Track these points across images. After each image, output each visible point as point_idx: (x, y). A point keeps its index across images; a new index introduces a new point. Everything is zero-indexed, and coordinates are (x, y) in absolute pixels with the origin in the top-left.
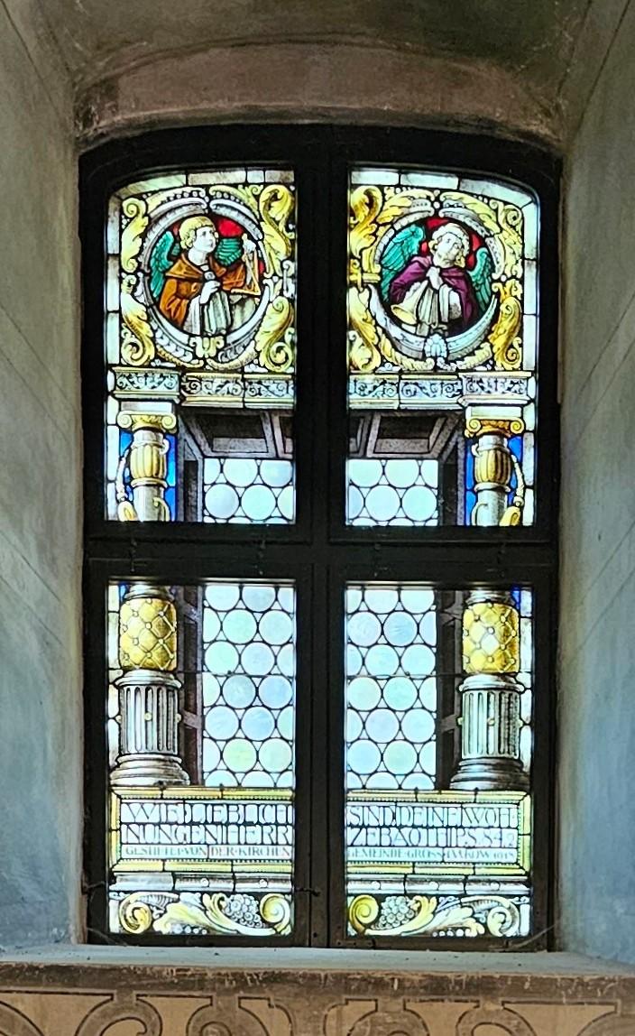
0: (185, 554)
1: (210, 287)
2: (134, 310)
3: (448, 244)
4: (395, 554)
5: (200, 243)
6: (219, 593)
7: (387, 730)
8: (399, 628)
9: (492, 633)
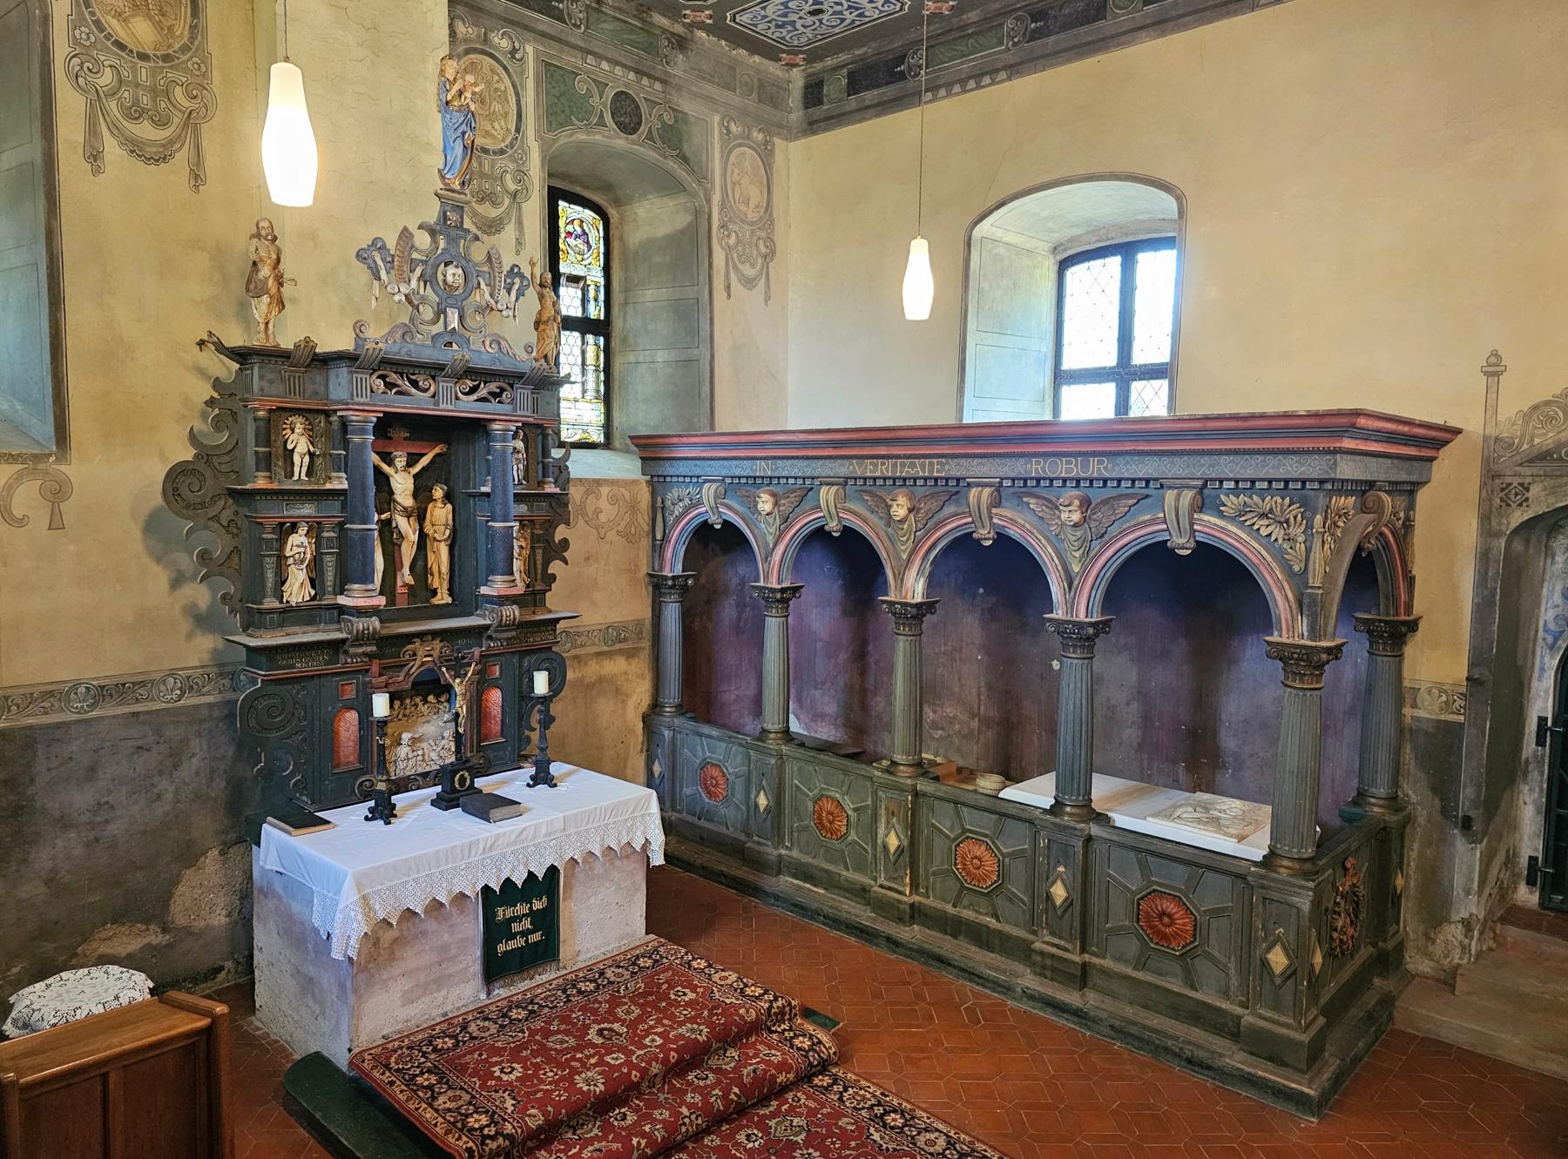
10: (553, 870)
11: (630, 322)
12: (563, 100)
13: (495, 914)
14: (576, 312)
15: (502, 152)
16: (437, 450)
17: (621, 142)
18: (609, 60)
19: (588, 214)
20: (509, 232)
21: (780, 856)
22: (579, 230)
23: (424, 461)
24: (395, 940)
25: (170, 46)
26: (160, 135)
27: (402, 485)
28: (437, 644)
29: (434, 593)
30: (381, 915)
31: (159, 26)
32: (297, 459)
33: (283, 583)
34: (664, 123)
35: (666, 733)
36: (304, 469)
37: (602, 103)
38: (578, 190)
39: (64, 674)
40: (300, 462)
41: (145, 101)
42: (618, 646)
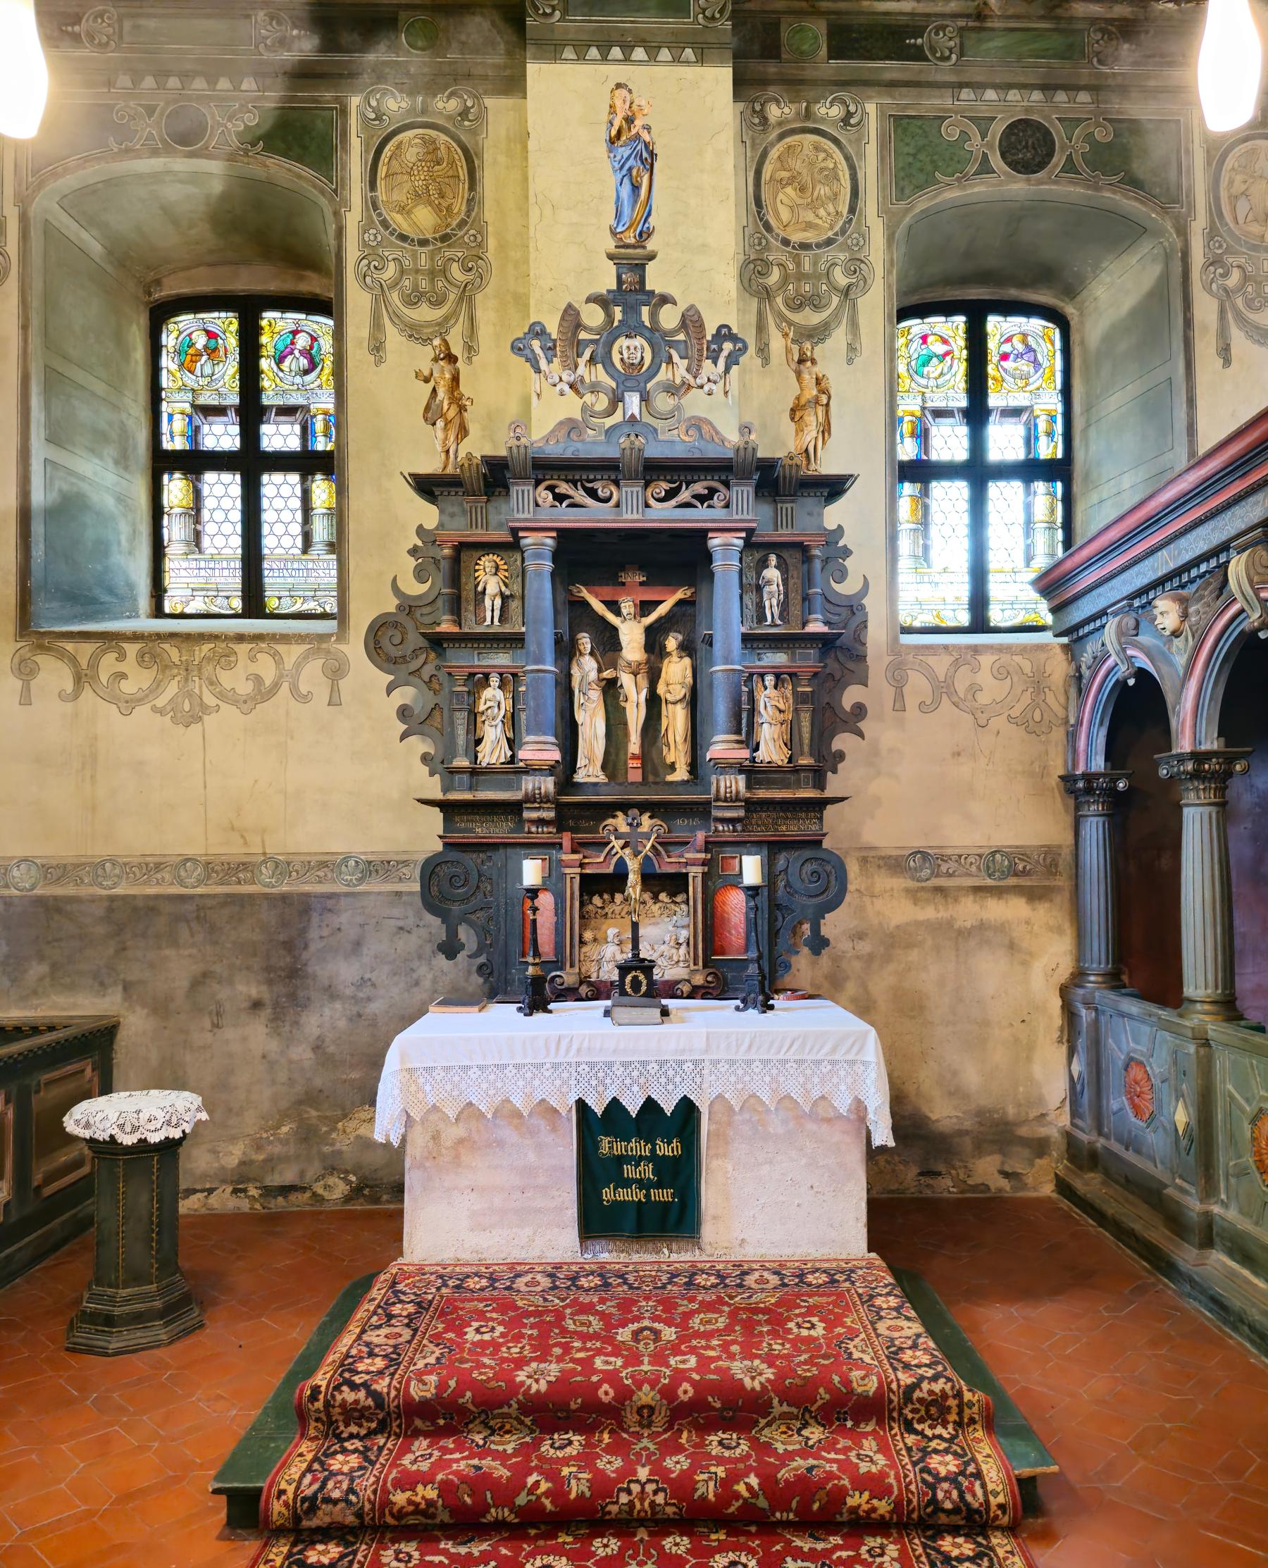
0: (195, 462)
1: (205, 358)
2: (173, 367)
3: (302, 341)
4: (282, 462)
5: (201, 341)
6: (210, 477)
7: (280, 531)
8: (286, 491)
9: (322, 490)
10: (687, 1108)
11: (1093, 448)
12: (922, 156)
13: (597, 1145)
14: (1017, 453)
15: (829, 242)
16: (680, 595)
17: (1019, 187)
18: (995, 87)
19: (1036, 324)
20: (839, 337)
21: (1208, 1215)
22: (1021, 347)
23: (662, 610)
24: (461, 1141)
25: (447, 226)
26: (437, 314)
27: (631, 635)
28: (646, 822)
29: (672, 767)
30: (431, 1100)
31: (438, 209)
32: (488, 603)
33: (478, 742)
35: (1083, 1012)
36: (497, 614)
37: (985, 145)
38: (1013, 293)
39: (337, 846)
40: (492, 604)
41: (424, 284)
42: (1012, 881)
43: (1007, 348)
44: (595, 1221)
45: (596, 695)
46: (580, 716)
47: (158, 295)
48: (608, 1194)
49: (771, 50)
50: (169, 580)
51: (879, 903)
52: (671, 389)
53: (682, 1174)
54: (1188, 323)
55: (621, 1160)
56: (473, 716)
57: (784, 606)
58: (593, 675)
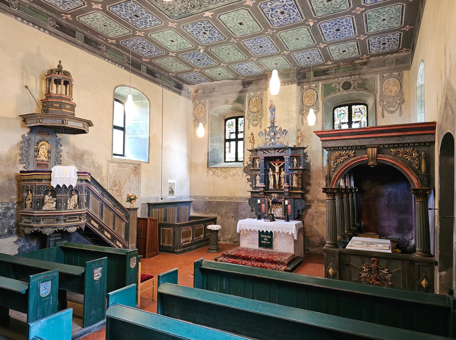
0: (230, 140)
5: (231, 123)
6: (231, 142)
17: (345, 92)
18: (341, 77)
19: (362, 106)
22: (359, 111)
23: (282, 164)
27: (277, 168)
28: (276, 195)
34: (359, 84)
37: (339, 87)
40: (258, 165)
43: (356, 111)
44: (261, 245)
45: (272, 176)
46: (270, 180)
47: (226, 118)
48: (262, 242)
49: (305, 78)
50: (226, 157)
51: (320, 208)
52: (278, 138)
53: (271, 240)
54: (376, 112)
55: (264, 238)
56: (255, 180)
57: (297, 165)
58: (271, 174)
